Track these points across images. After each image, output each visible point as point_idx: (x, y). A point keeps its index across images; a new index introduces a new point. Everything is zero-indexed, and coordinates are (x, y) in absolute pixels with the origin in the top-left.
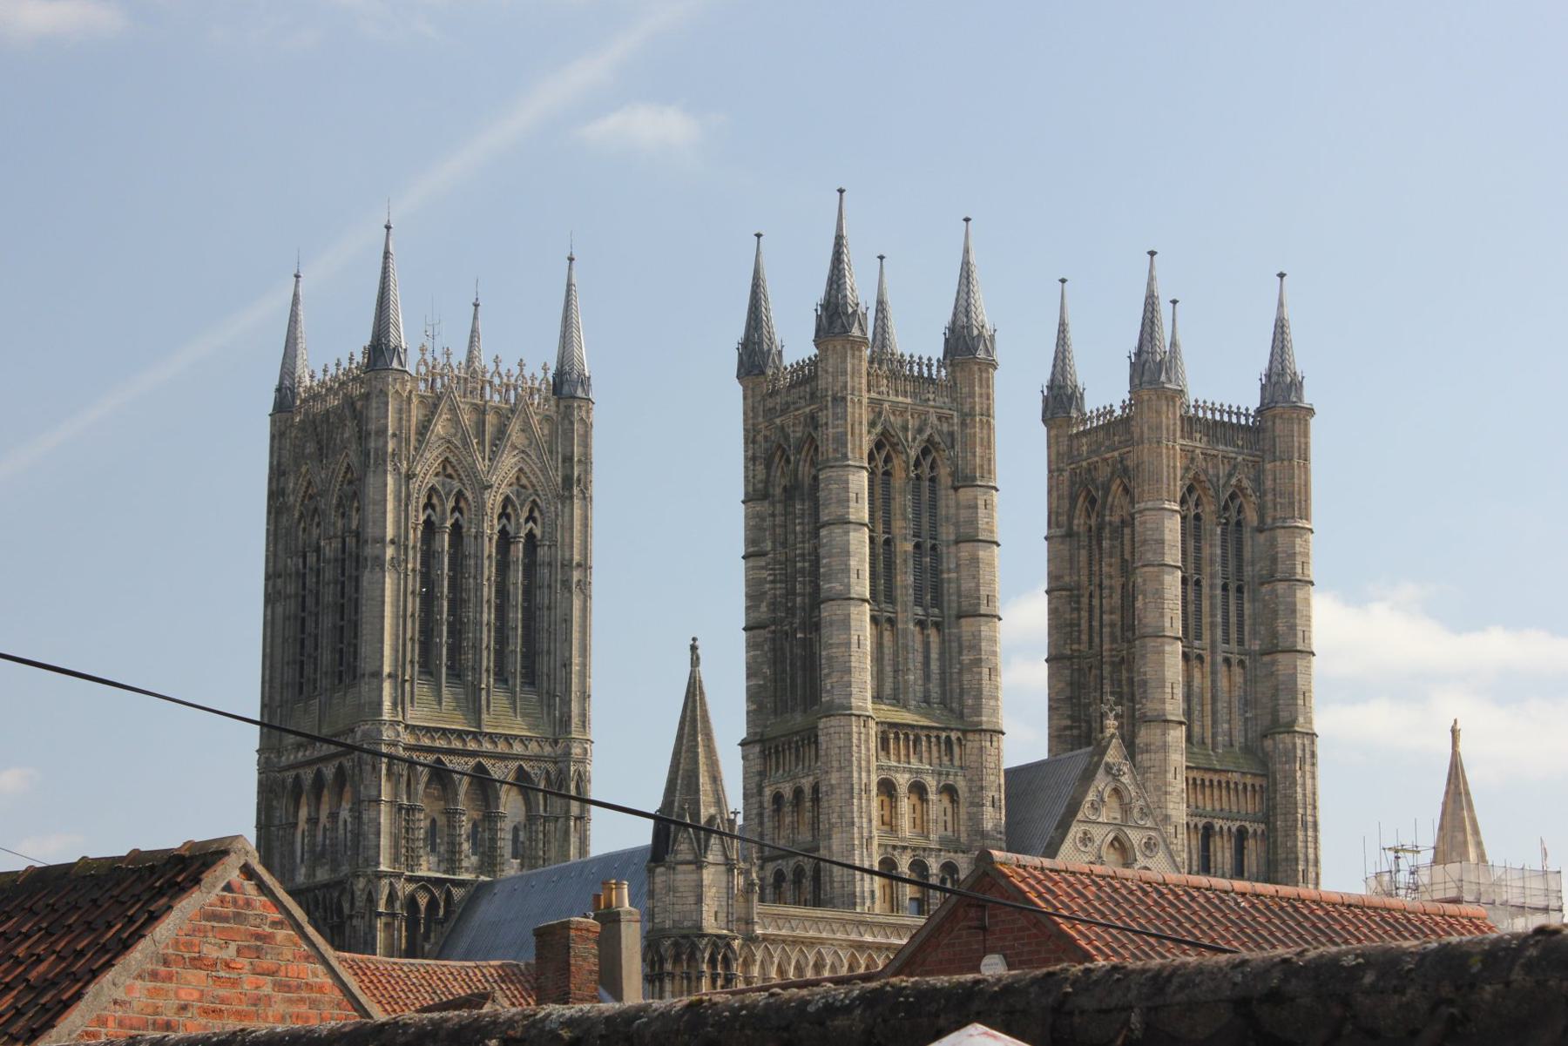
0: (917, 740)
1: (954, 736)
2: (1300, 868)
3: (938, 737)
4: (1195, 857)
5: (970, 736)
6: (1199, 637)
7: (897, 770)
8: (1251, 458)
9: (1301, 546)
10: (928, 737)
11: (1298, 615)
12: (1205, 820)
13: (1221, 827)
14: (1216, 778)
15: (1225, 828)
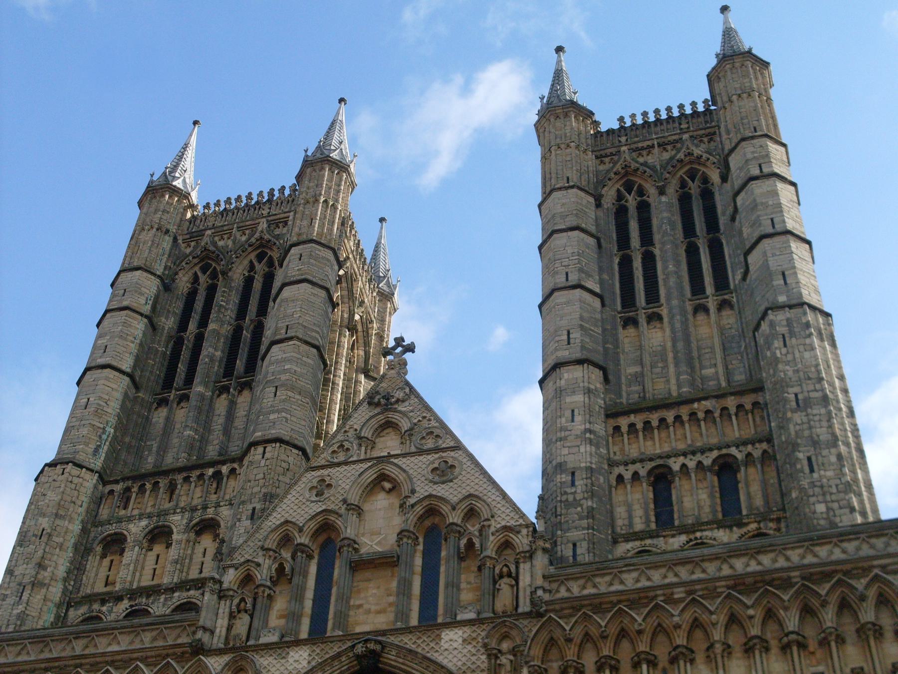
0: (172, 489)
1: (225, 469)
2: (801, 455)
3: (201, 477)
4: (638, 512)
5: (246, 462)
6: (652, 295)
7: (130, 519)
8: (703, 132)
9: (753, 152)
10: (187, 479)
11: (760, 207)
12: (649, 465)
13: (684, 466)
14: (670, 416)
15: (691, 464)
